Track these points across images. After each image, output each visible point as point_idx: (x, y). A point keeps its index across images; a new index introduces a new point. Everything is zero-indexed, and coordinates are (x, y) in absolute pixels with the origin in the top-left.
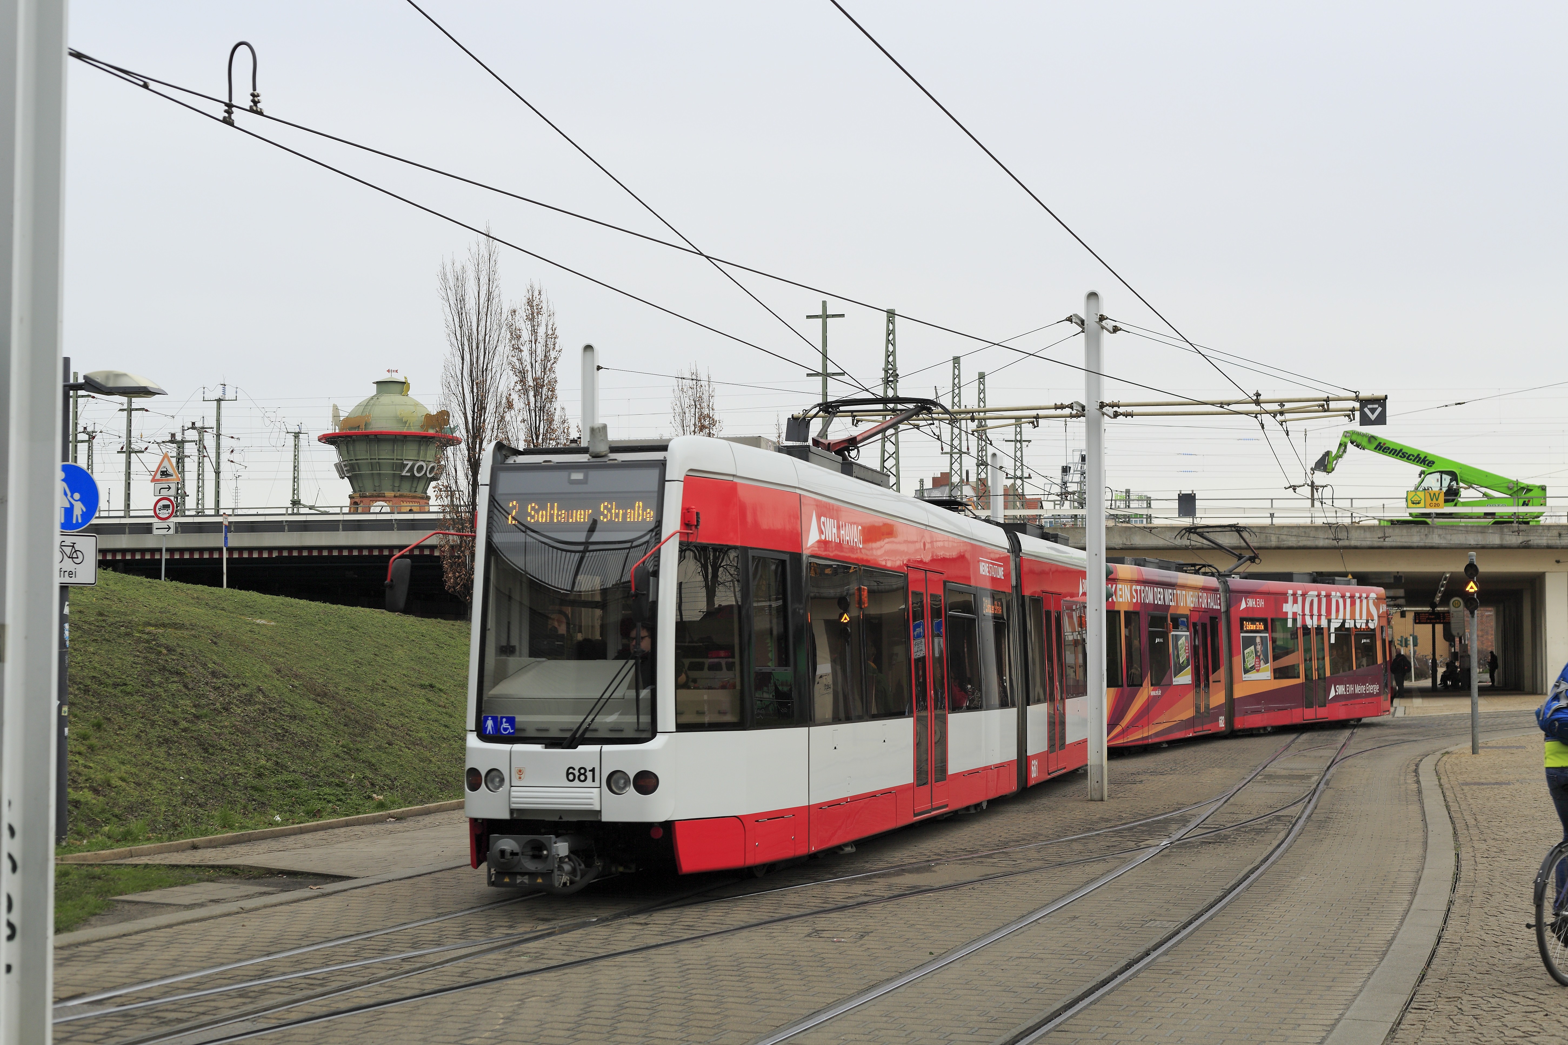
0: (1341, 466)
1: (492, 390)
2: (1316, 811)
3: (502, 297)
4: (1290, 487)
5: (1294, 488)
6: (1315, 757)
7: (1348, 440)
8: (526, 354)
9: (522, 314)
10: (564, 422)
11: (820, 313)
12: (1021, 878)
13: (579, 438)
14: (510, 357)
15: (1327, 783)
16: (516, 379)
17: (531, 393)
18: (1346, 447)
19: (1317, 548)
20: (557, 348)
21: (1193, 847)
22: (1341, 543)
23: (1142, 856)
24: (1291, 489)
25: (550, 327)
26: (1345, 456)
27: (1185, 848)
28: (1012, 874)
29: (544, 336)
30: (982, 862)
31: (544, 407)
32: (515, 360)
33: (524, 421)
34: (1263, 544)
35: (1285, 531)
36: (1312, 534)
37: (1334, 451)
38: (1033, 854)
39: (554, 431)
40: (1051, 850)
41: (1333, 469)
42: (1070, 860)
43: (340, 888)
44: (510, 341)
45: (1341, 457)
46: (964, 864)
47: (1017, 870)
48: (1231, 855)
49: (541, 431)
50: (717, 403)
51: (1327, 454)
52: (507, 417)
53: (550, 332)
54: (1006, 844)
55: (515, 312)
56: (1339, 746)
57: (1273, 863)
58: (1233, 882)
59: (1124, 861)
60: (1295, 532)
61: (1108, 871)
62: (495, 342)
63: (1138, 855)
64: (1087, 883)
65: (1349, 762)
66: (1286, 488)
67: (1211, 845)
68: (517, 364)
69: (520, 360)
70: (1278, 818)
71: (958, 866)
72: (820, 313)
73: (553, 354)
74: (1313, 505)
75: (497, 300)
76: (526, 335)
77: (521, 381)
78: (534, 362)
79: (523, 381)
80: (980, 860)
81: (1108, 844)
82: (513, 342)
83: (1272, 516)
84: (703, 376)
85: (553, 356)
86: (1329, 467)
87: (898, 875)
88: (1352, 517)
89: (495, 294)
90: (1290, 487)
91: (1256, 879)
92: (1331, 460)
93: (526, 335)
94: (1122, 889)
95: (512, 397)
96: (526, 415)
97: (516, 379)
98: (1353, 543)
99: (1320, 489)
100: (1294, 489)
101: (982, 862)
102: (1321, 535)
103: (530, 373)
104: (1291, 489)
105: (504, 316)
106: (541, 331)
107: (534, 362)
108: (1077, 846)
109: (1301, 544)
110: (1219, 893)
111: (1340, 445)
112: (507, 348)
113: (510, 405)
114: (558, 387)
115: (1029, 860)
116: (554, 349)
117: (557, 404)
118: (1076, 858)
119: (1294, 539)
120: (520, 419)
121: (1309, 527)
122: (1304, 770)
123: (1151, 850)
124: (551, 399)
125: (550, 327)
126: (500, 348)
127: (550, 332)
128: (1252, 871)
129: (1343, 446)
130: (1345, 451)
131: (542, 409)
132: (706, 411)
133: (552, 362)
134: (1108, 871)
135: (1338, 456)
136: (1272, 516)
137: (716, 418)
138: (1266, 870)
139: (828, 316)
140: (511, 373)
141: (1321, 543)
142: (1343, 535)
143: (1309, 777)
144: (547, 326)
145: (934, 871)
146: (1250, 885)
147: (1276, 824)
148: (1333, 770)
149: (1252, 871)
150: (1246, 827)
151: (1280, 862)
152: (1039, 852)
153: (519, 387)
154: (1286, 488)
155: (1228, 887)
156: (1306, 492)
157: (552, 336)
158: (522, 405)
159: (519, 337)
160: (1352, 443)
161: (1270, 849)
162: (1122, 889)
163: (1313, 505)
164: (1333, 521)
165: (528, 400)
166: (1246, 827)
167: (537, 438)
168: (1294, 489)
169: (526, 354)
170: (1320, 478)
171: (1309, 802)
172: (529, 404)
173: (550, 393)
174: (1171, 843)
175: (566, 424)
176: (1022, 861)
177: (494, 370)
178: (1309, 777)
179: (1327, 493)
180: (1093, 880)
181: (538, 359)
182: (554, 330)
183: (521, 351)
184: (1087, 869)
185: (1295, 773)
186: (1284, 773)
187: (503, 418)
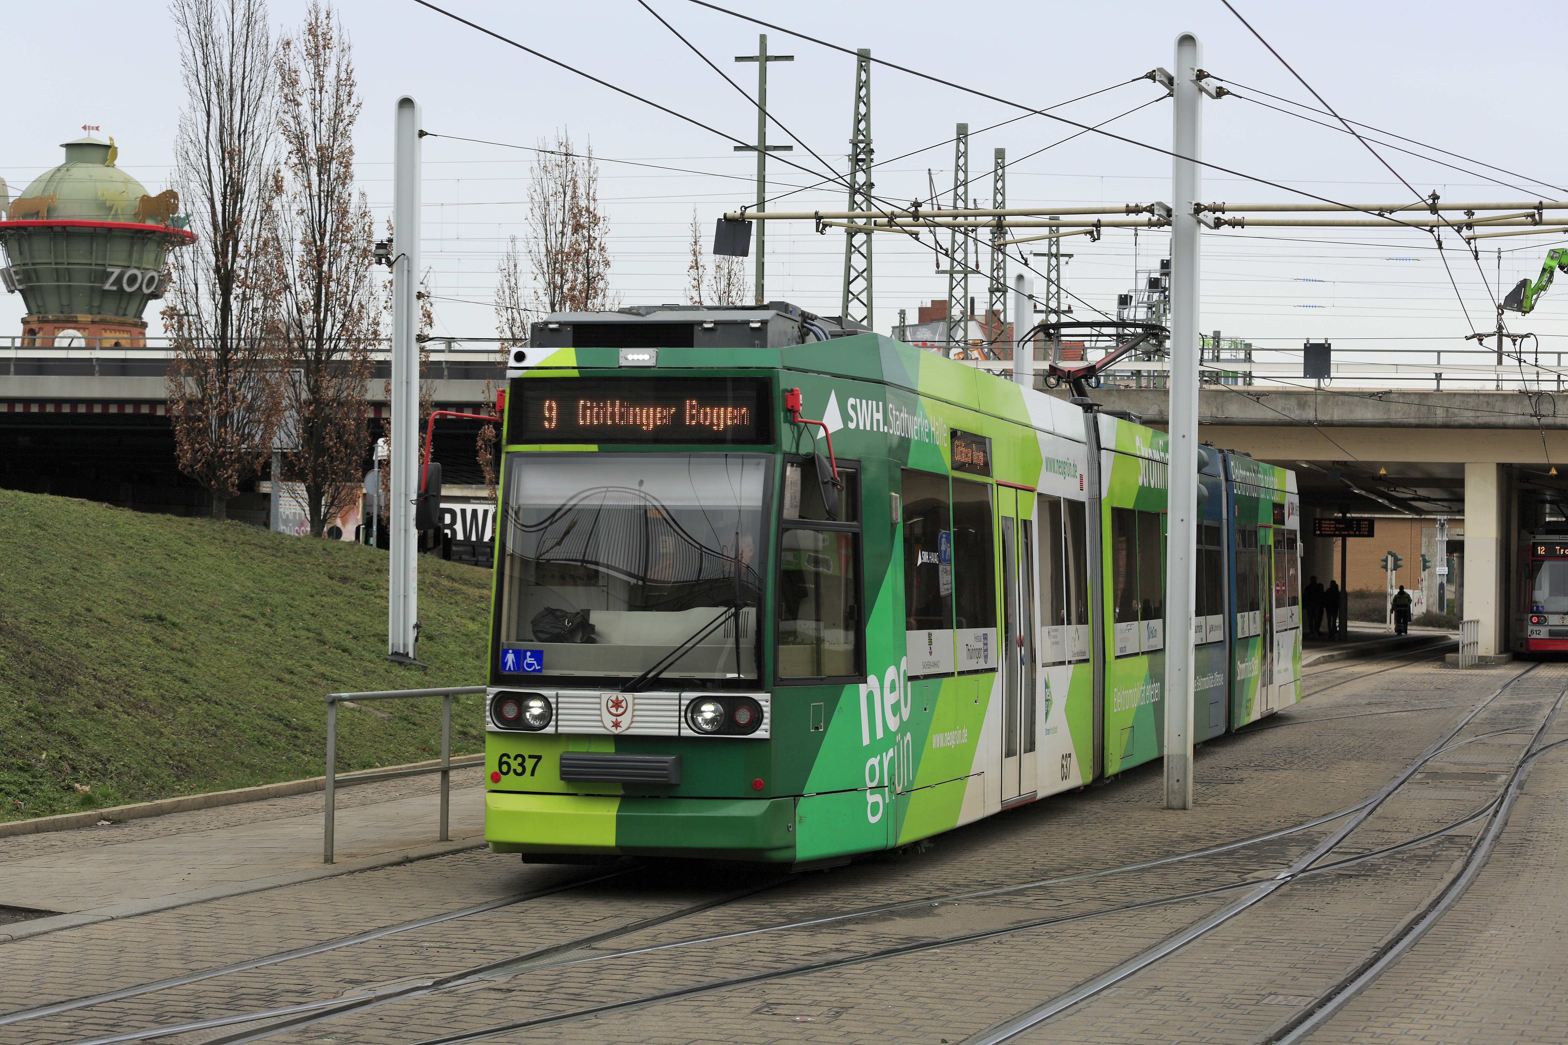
0: (1543, 304)
1: (253, 163)
2: (1507, 829)
3: (269, 20)
4: (1473, 337)
5: (1480, 337)
6: (1501, 746)
7: (1555, 264)
8: (305, 109)
9: (300, 45)
10: (364, 215)
11: (756, 53)
12: (1071, 927)
13: (390, 240)
14: (281, 114)
15: (1521, 786)
16: (290, 147)
17: (314, 170)
18: (1552, 273)
19: (1505, 427)
20: (354, 101)
21: (1326, 881)
22: (1544, 421)
23: (1251, 896)
24: (1475, 340)
25: (343, 68)
26: (1551, 288)
27: (1315, 884)
28: (1056, 920)
29: (334, 83)
30: (1010, 902)
31: (333, 192)
32: (288, 118)
33: (302, 212)
34: (1424, 421)
35: (1457, 402)
36: (1499, 405)
37: (1535, 281)
38: (1088, 891)
39: (348, 228)
40: (1112, 885)
41: (1532, 308)
42: (1142, 900)
43: (38, 930)
44: (281, 88)
45: (1544, 288)
46: (983, 904)
47: (1064, 914)
48: (1384, 895)
49: (328, 228)
50: (601, 189)
51: (1524, 283)
52: (276, 205)
53: (343, 76)
54: (1044, 874)
55: (288, 44)
56: (1536, 729)
57: (1447, 908)
58: (1390, 937)
59: (1224, 903)
60: (1472, 402)
61: (1201, 918)
62: (259, 89)
63: (1245, 893)
64: (1171, 936)
65: (1552, 754)
66: (1467, 338)
67: (1353, 880)
68: (292, 124)
69: (296, 118)
70: (1451, 839)
71: (973, 907)
72: (756, 53)
73: (347, 110)
74: (1500, 362)
75: (261, 24)
76: (306, 80)
77: (299, 150)
78: (318, 122)
79: (301, 151)
80: (1006, 898)
81: (1198, 876)
82: (286, 90)
83: (1438, 377)
84: (578, 148)
85: (347, 113)
86: (1526, 304)
87: (885, 920)
88: (1559, 380)
89: (259, 15)
90: (1473, 337)
91: (1424, 932)
92: (1529, 293)
93: (306, 80)
94: (1223, 946)
95: (281, 174)
96: (306, 205)
97: (290, 147)
98: (1559, 421)
99: (1519, 340)
100: (1480, 340)
101: (1010, 902)
102: (1512, 408)
103: (311, 139)
104: (1475, 340)
105: (272, 50)
106: (330, 74)
107: (318, 122)
108: (1151, 879)
109: (1481, 420)
110: (1369, 954)
111: (1544, 270)
112: (277, 99)
113: (279, 188)
114: (354, 160)
115: (1081, 900)
116: (349, 101)
117: (354, 187)
118: (1151, 897)
119: (1471, 414)
120: (295, 207)
121: (1493, 395)
122: (1485, 765)
123: (1263, 885)
124: (344, 178)
125: (343, 68)
126: (266, 100)
127: (343, 76)
128: (1416, 921)
129: (1547, 273)
130: (1550, 280)
131: (330, 194)
132: (583, 203)
133: (346, 122)
134: (1201, 918)
135: (1541, 288)
136: (1438, 377)
137: (599, 213)
138: (1437, 919)
139: (768, 59)
140: (282, 138)
141: (1511, 420)
142: (1546, 408)
143: (1493, 776)
144: (338, 66)
145: (938, 915)
146: (1415, 942)
147: (1448, 849)
148: (1529, 766)
149: (1416, 921)
150: (1404, 852)
151: (1457, 907)
152: (1095, 887)
153: (294, 160)
154: (1467, 338)
155: (1382, 944)
156: (1491, 343)
157: (346, 83)
158: (299, 188)
159: (294, 83)
160: (1562, 267)
161: (1442, 886)
162: (1223, 946)
163: (1500, 362)
164: (1534, 387)
165: (309, 180)
166: (1404, 852)
167: (322, 240)
168: (1480, 340)
169: (305, 109)
170: (1514, 321)
171: (1495, 815)
172: (309, 186)
173: (342, 170)
174: (1292, 876)
175: (367, 219)
176: (1070, 901)
177: (256, 133)
178: (1493, 776)
179: (1528, 345)
180: (1179, 932)
181: (324, 117)
182: (349, 73)
183: (298, 104)
184: (1170, 914)
185: (1472, 769)
186: (1455, 769)
187: (269, 208)
